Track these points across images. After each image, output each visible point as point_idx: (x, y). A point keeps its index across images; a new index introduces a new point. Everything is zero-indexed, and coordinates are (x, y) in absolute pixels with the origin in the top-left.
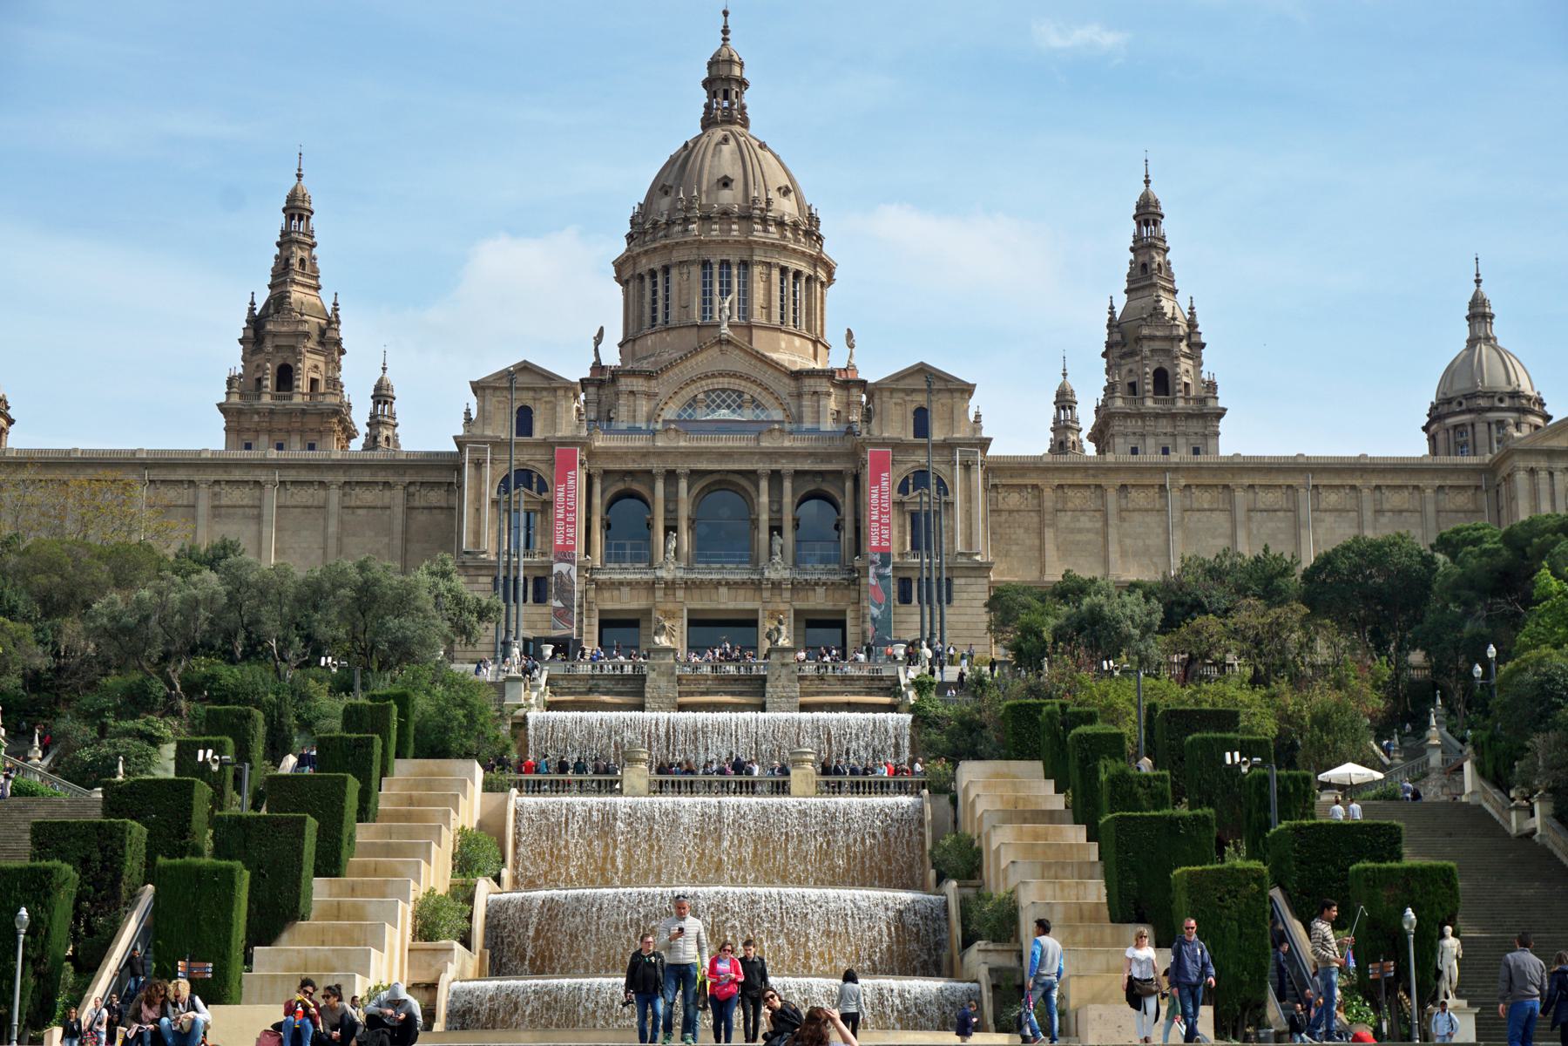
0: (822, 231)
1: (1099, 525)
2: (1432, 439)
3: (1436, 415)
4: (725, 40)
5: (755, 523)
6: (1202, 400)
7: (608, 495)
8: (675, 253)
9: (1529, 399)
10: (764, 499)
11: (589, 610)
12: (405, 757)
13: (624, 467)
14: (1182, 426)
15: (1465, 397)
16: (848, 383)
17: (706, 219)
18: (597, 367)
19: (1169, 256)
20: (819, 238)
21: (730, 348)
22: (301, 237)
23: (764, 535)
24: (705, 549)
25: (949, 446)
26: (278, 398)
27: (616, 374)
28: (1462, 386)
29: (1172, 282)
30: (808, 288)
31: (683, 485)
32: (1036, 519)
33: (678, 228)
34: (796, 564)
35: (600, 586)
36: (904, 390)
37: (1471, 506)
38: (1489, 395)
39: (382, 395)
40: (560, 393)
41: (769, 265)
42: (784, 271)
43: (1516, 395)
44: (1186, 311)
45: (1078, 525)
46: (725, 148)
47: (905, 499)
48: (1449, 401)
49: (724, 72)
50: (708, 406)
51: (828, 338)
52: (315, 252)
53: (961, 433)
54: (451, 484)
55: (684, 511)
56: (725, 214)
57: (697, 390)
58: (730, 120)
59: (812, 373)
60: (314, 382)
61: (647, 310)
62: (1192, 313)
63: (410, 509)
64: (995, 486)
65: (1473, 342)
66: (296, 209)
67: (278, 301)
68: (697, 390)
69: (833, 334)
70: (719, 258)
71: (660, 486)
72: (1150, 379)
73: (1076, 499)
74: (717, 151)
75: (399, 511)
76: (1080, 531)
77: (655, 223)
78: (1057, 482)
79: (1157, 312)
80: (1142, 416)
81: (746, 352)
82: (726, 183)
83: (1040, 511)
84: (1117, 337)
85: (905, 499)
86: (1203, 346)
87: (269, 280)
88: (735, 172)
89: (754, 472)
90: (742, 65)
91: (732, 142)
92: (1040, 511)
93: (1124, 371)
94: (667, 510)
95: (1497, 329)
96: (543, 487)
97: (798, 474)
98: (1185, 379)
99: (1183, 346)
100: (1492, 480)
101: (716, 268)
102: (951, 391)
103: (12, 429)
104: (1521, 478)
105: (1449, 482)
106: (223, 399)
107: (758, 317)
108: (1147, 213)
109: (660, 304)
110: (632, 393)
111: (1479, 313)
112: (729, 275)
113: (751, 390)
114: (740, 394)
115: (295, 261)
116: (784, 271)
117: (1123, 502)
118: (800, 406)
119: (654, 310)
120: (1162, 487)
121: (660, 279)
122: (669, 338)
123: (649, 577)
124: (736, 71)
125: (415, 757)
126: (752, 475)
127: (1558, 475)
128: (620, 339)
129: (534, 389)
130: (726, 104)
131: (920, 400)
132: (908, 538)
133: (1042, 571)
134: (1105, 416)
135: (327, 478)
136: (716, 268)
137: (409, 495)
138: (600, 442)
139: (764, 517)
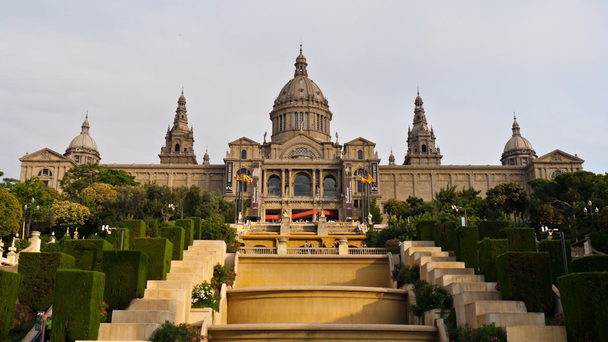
0: (329, 105)
1: (412, 185)
2: (503, 163)
3: (504, 157)
5: (311, 185)
6: (436, 153)
7: (268, 176)
8: (287, 110)
9: (532, 151)
10: (314, 177)
11: (263, 209)
12: (198, 239)
13: (273, 168)
15: (513, 151)
16: (337, 146)
17: (296, 100)
18: (265, 142)
20: (328, 106)
21: (303, 136)
22: (183, 110)
24: (299, 191)
25: (368, 161)
26: (176, 153)
27: (270, 144)
28: (512, 147)
29: (426, 121)
30: (325, 120)
31: (290, 173)
32: (393, 184)
33: (288, 103)
34: (324, 197)
35: (266, 202)
36: (354, 145)
37: (520, 180)
39: (206, 158)
40: (254, 146)
41: (314, 113)
43: (528, 150)
44: (430, 129)
45: (406, 185)
47: (356, 177)
48: (508, 152)
49: (301, 61)
50: (297, 153)
51: (331, 134)
52: (186, 113)
53: (372, 158)
54: (223, 174)
55: (291, 180)
56: (302, 99)
57: (294, 148)
58: (303, 74)
60: (185, 149)
61: (279, 126)
62: (432, 130)
64: (381, 174)
66: (182, 102)
67: (176, 127)
68: (294, 148)
69: (332, 134)
70: (300, 111)
71: (284, 174)
72: (421, 147)
73: (405, 177)
74: (299, 81)
76: (406, 187)
77: (282, 103)
78: (399, 173)
79: (422, 129)
80: (419, 158)
81: (309, 138)
82: (302, 90)
83: (395, 182)
84: (411, 136)
85: (356, 177)
86: (435, 139)
87: (174, 121)
88: (305, 88)
89: (311, 169)
90: (306, 59)
91: (303, 79)
92: (395, 182)
93: (413, 145)
94: (286, 181)
95: (521, 132)
97: (324, 170)
98: (431, 148)
100: (528, 170)
101: (299, 114)
102: (369, 145)
103: (100, 161)
104: (537, 171)
105: (514, 173)
106: (160, 153)
107: (311, 127)
108: (418, 102)
109: (283, 124)
110: (275, 149)
111: (515, 128)
112: (303, 116)
115: (181, 116)
116: (318, 115)
117: (419, 179)
118: (323, 152)
119: (281, 126)
120: (430, 174)
121: (283, 117)
123: (280, 200)
124: (304, 61)
125: (202, 239)
126: (311, 171)
128: (271, 135)
129: (247, 145)
130: (301, 70)
131: (360, 148)
132: (357, 188)
133: (395, 197)
134: (408, 160)
135: (187, 171)
136: (299, 114)
137: (211, 177)
138: (266, 161)
139: (314, 183)
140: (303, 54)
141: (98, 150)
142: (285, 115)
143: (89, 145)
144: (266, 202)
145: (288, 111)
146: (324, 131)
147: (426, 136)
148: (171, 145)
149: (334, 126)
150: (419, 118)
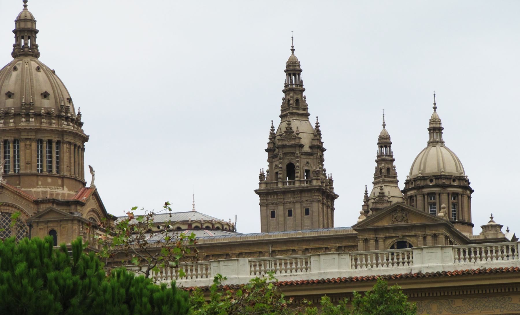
4: (25, 6)
14: (298, 197)
19: (305, 93)
21: (4, 191)
28: (416, 172)
29: (306, 109)
42: (41, 141)
46: (14, 74)
49: (22, 25)
62: (318, 126)
65: (429, 143)
82: (9, 95)
90: (33, 21)
108: (293, 69)
114: (10, 214)
127: (381, 242)
131: (51, 226)
146: (55, 170)
147: (294, 146)
150: (294, 102)
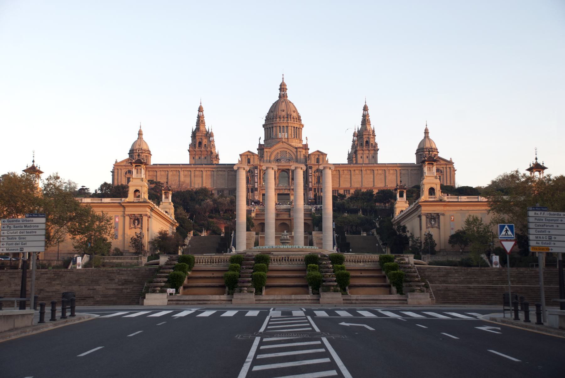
5: (289, 178)
17: (280, 118)
18: (260, 145)
23: (291, 180)
28: (422, 146)
29: (370, 122)
38: (427, 149)
43: (431, 148)
49: (283, 87)
51: (303, 139)
57: (278, 151)
59: (300, 148)
63: (228, 175)
65: (425, 137)
67: (198, 129)
72: (365, 143)
75: (226, 175)
83: (339, 175)
88: (285, 109)
92: (339, 175)
96: (252, 173)
99: (372, 136)
108: (365, 108)
113: (288, 151)
122: (273, 140)
140: (285, 81)
141: (150, 149)
142: (272, 127)
143: (144, 147)
144: (262, 190)
145: (274, 125)
147: (369, 135)
148: (195, 142)
149: (305, 133)
150: (365, 120)
